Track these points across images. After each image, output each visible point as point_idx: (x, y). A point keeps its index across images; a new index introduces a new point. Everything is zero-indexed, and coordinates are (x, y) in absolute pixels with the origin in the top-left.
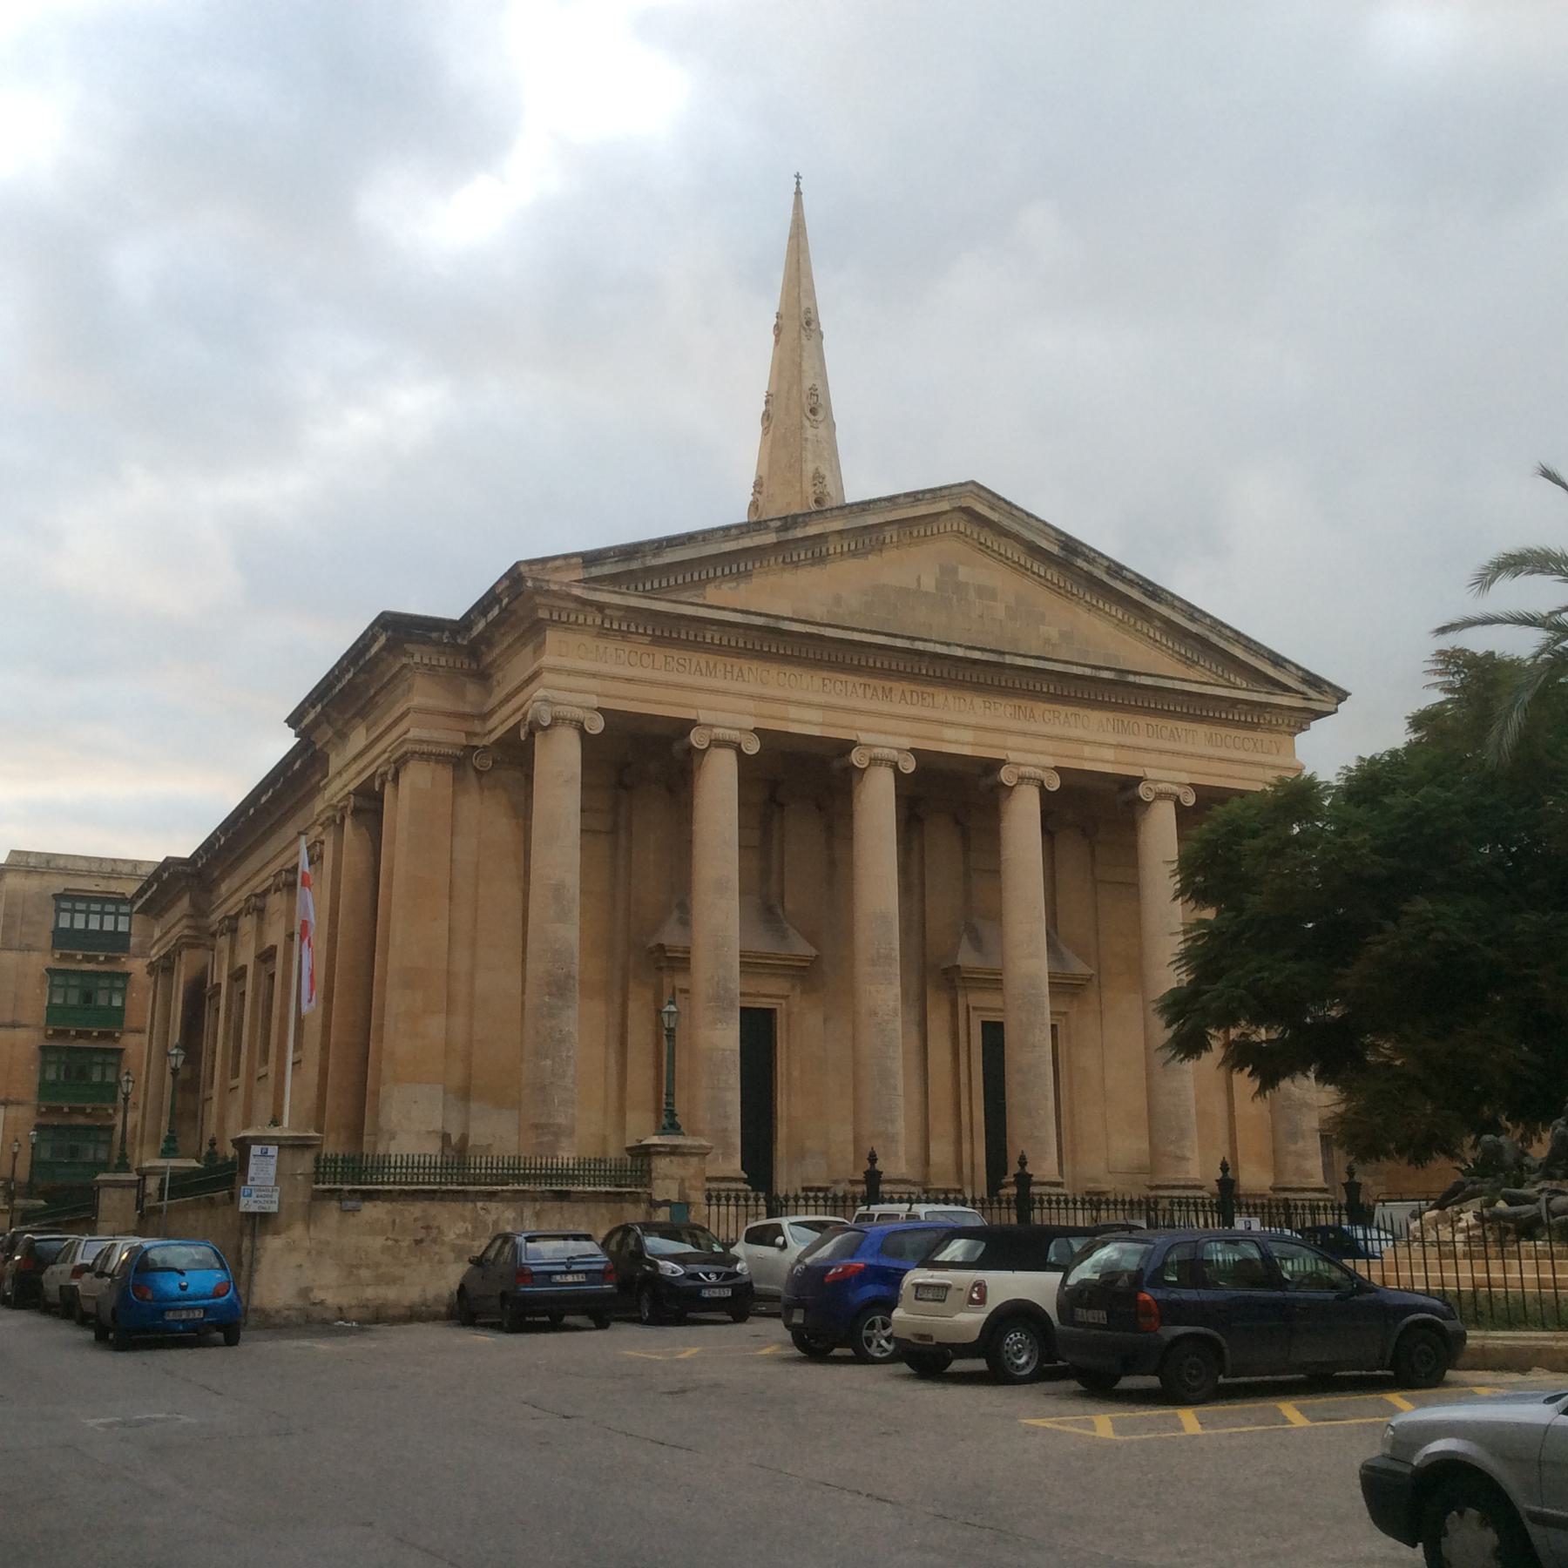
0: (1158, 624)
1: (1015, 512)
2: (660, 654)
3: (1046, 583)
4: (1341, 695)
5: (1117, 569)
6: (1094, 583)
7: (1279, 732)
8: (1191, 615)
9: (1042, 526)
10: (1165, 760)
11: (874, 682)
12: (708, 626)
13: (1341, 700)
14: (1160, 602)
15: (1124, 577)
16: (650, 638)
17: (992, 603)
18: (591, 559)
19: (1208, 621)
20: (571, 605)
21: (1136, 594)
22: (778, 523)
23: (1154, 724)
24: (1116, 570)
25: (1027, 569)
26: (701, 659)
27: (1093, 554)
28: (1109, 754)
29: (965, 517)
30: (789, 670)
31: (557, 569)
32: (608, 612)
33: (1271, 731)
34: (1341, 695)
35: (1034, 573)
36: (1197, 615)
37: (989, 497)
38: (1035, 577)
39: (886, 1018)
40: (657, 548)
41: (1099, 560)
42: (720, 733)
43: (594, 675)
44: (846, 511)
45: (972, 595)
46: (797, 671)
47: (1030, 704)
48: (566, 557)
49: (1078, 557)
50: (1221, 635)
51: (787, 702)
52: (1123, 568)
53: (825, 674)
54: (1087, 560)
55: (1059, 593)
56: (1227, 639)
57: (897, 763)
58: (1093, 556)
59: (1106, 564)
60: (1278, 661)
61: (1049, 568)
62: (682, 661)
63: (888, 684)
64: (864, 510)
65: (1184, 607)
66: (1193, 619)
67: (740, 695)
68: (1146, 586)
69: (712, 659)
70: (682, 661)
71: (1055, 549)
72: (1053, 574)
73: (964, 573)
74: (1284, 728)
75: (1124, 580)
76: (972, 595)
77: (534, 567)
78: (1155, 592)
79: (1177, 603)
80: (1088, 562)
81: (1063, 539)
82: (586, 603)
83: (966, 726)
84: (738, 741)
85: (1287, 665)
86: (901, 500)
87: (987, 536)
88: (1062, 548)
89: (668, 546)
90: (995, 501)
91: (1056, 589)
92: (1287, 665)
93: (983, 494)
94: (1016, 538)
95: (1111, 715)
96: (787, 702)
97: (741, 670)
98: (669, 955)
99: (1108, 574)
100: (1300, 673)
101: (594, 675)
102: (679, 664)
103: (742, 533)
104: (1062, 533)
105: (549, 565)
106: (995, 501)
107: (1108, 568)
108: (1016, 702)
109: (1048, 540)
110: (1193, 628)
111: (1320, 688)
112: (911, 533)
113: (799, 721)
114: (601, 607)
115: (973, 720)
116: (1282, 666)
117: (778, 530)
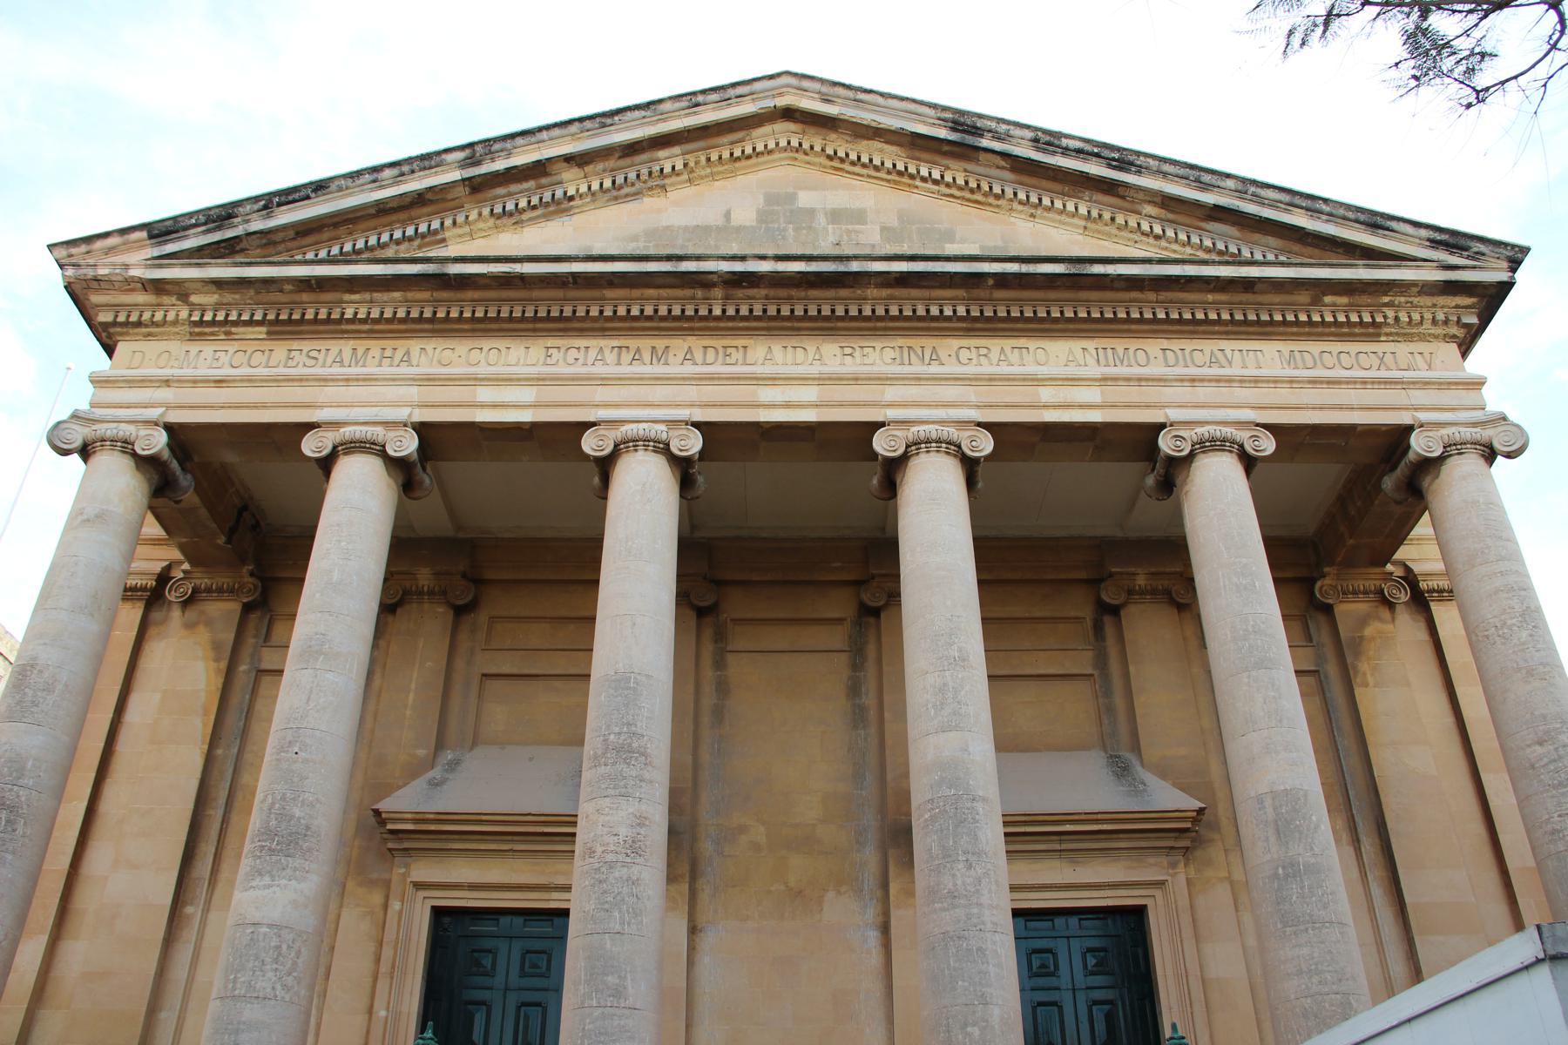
0: (1149, 209)
1: (861, 96)
2: (280, 350)
3: (948, 191)
4: (1515, 256)
5: (1048, 138)
6: (1023, 167)
7: (1423, 338)
8: (1197, 180)
9: (912, 107)
10: (1203, 393)
11: (633, 343)
12: (347, 297)
13: (1515, 264)
14: (1139, 173)
15: (1067, 149)
16: (264, 329)
17: (857, 227)
18: (160, 231)
19: (1230, 183)
20: (141, 298)
21: (1095, 169)
22: (460, 155)
23: (1175, 348)
24: (1048, 140)
25: (912, 177)
26: (346, 347)
27: (1004, 127)
28: (1092, 394)
29: (792, 126)
30: (486, 344)
31: (110, 251)
32: (194, 299)
33: (1408, 337)
34: (1515, 256)
35: (924, 179)
36: (1206, 178)
37: (817, 86)
38: (929, 185)
39: (610, 857)
40: (266, 207)
41: (1017, 132)
42: (348, 432)
43: (167, 383)
44: (574, 128)
45: (821, 220)
46: (501, 343)
47: (929, 342)
48: (123, 232)
49: (981, 136)
50: (1259, 200)
51: (476, 380)
52: (1060, 135)
53: (550, 342)
54: (998, 137)
55: (976, 202)
56: (1273, 205)
57: (668, 445)
58: (1005, 128)
59: (1029, 134)
60: (1376, 221)
61: (948, 168)
62: (314, 354)
63: (660, 343)
64: (604, 126)
65: (1182, 172)
66: (1205, 187)
67: (393, 380)
68: (1106, 153)
69: (361, 345)
70: (314, 354)
71: (943, 133)
72: (956, 172)
73: (805, 199)
74: (1427, 327)
75: (1066, 151)
76: (821, 220)
77: (74, 251)
78: (1124, 159)
79: (1167, 168)
80: (999, 139)
81: (949, 115)
82: (158, 287)
83: (803, 380)
84: (380, 439)
85: (1394, 225)
86: (667, 106)
87: (838, 144)
88: (954, 129)
89: (279, 205)
90: (825, 89)
91: (971, 195)
92: (1394, 225)
93: (806, 84)
94: (876, 133)
95: (1091, 344)
96: (476, 380)
97: (408, 353)
98: (389, 827)
99: (1038, 149)
100: (1424, 233)
101: (167, 383)
102: (309, 356)
103: (402, 174)
104: (945, 109)
105: (99, 244)
106: (825, 89)
107: (1036, 140)
108: (900, 341)
109: (924, 122)
110: (1209, 198)
111: (1466, 249)
112: (709, 159)
113: (495, 406)
114: (180, 290)
115: (815, 370)
116: (1387, 229)
117: (464, 164)
